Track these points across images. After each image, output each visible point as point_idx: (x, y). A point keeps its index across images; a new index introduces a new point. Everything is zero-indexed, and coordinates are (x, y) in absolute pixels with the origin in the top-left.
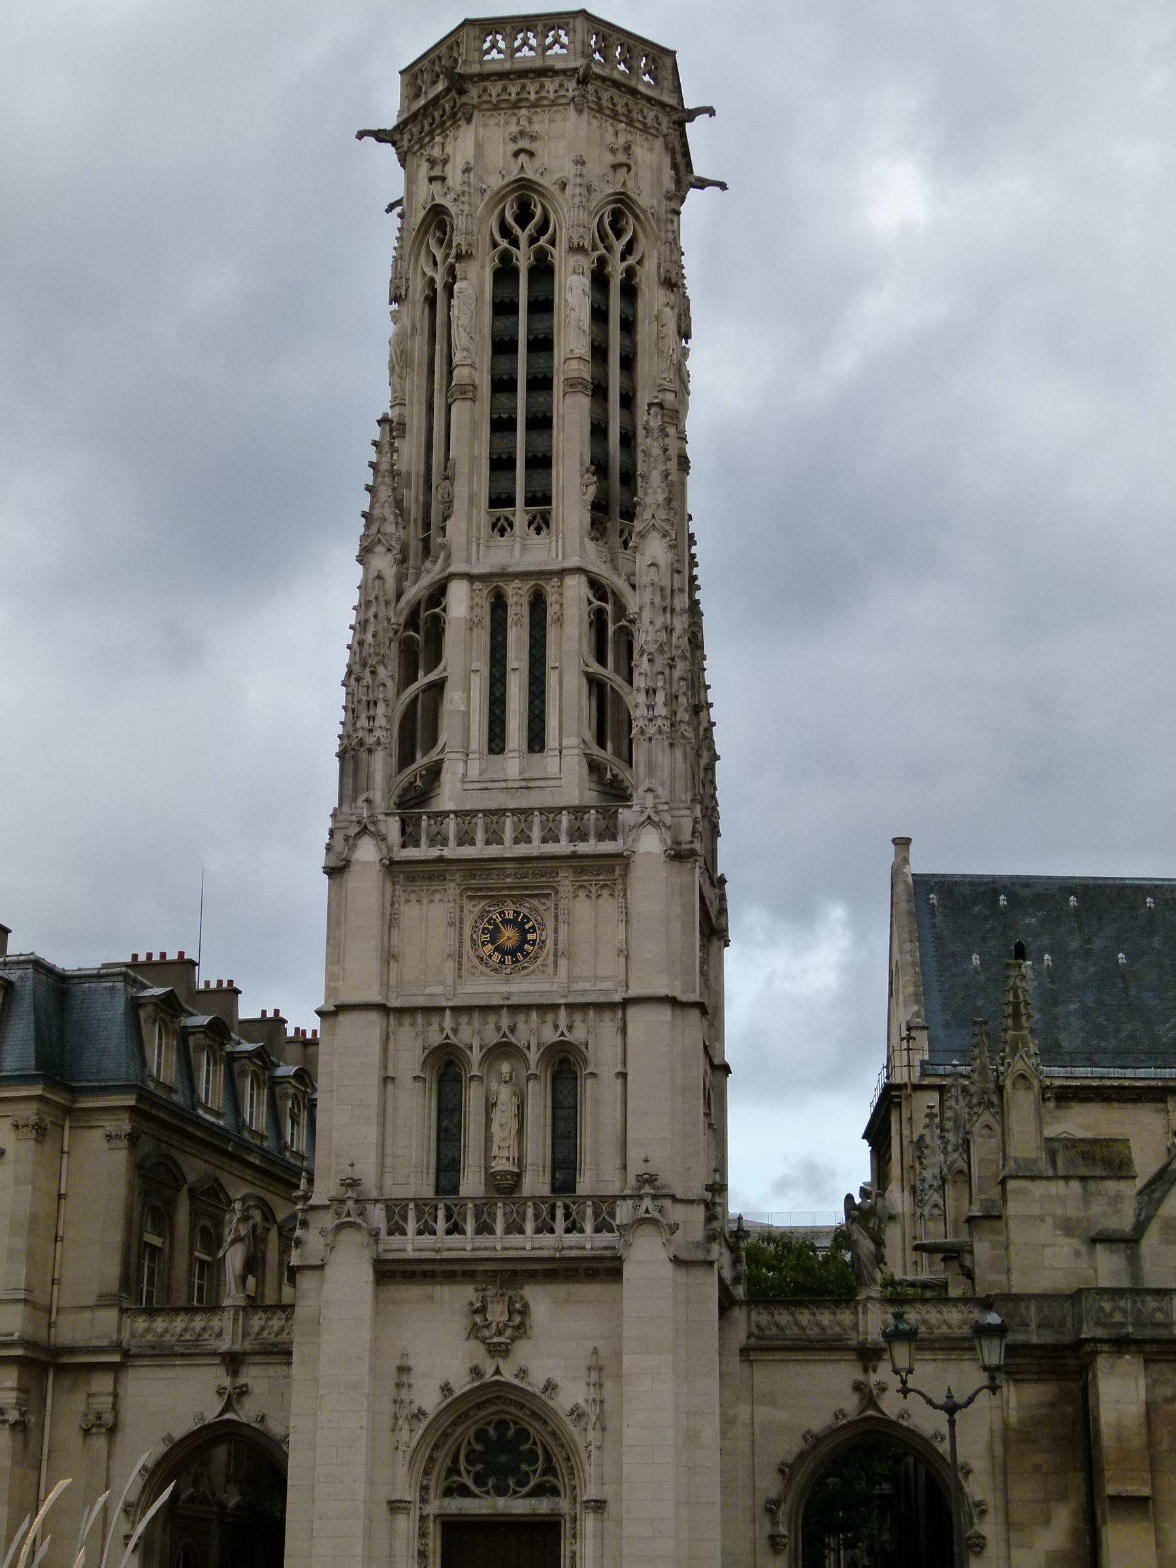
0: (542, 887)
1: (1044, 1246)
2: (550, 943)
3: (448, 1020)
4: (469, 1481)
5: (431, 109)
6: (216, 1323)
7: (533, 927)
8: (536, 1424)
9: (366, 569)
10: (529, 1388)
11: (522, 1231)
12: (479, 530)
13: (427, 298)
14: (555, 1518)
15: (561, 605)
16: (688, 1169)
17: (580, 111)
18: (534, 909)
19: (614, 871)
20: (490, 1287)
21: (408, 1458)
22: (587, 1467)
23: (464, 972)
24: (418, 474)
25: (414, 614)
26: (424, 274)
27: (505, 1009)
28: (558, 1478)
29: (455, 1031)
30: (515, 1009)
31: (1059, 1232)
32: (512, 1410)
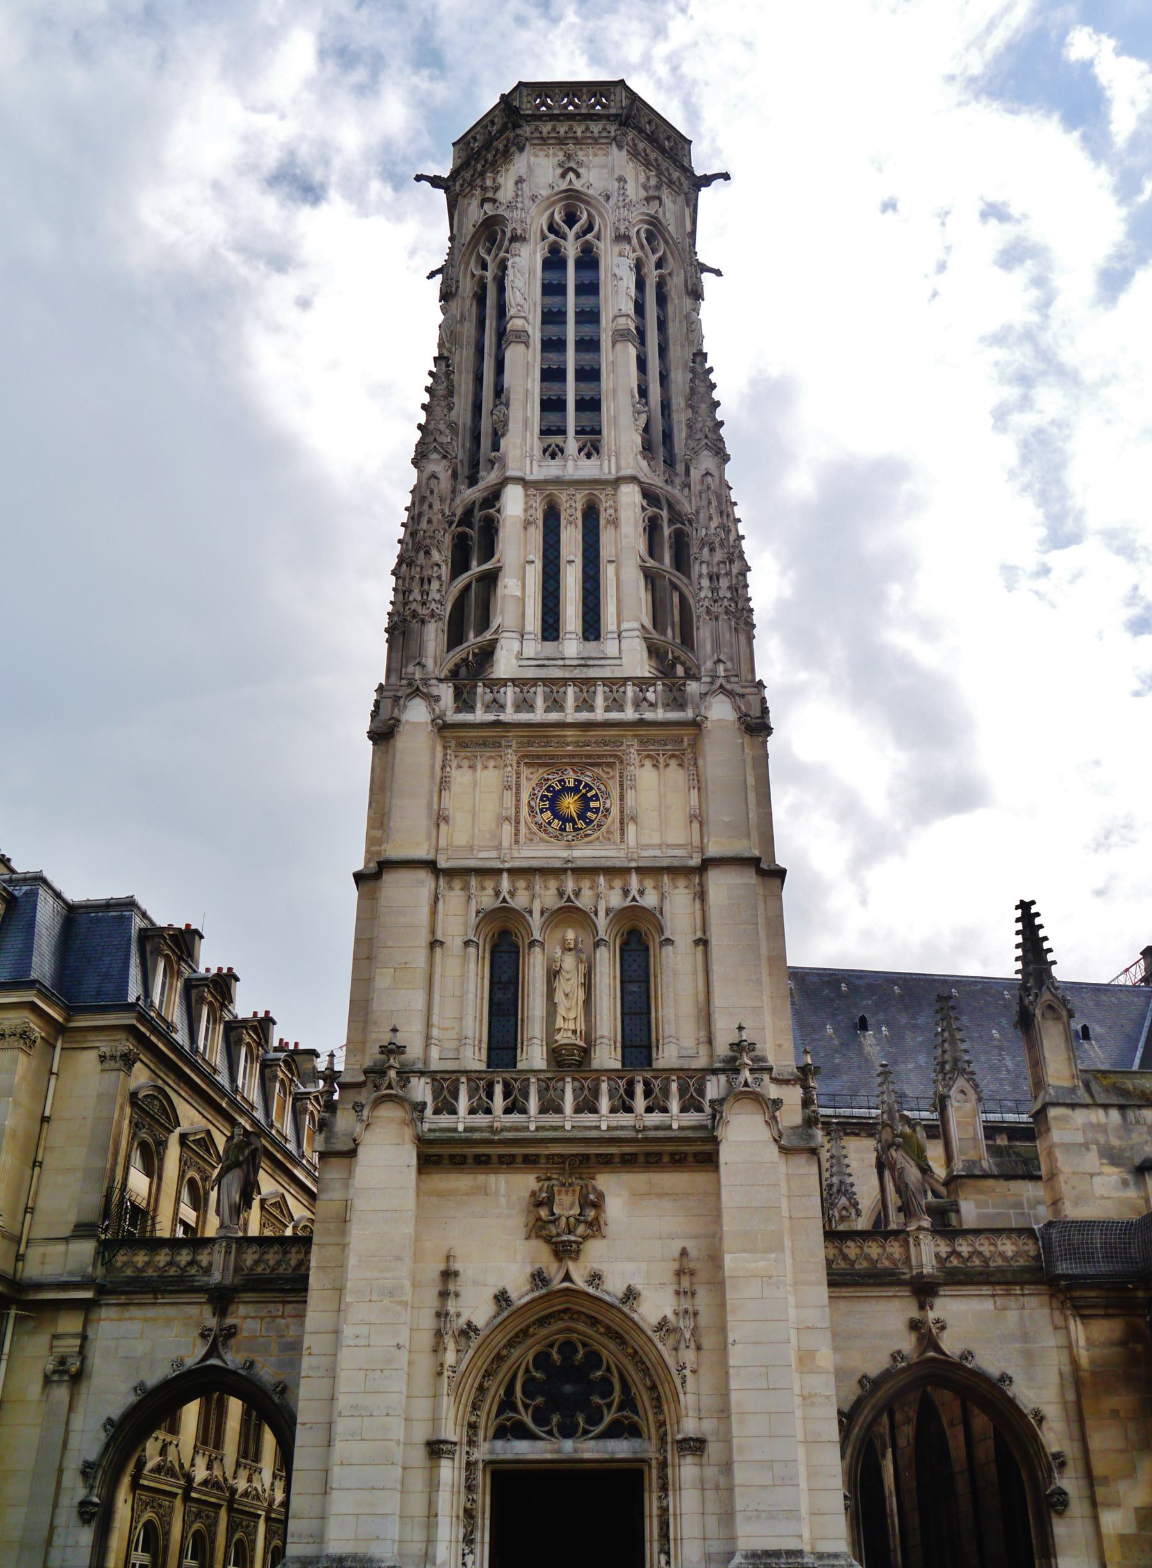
0: (606, 756)
1: (1092, 1175)
2: (615, 812)
3: (505, 883)
4: (528, 1420)
5: (484, 153)
6: (204, 1258)
7: (596, 795)
8: (612, 1345)
9: (420, 471)
10: (607, 1298)
11: (594, 1110)
12: (532, 449)
13: (475, 295)
14: (636, 1465)
15: (616, 510)
16: (780, 1046)
17: (620, 147)
18: (599, 779)
19: (682, 741)
20: (555, 1176)
21: (452, 1384)
22: (681, 1396)
23: (522, 839)
24: (464, 425)
25: (468, 513)
26: (473, 275)
27: (569, 872)
28: (637, 1413)
29: (512, 894)
30: (580, 872)
31: (1105, 1161)
32: (581, 1327)
